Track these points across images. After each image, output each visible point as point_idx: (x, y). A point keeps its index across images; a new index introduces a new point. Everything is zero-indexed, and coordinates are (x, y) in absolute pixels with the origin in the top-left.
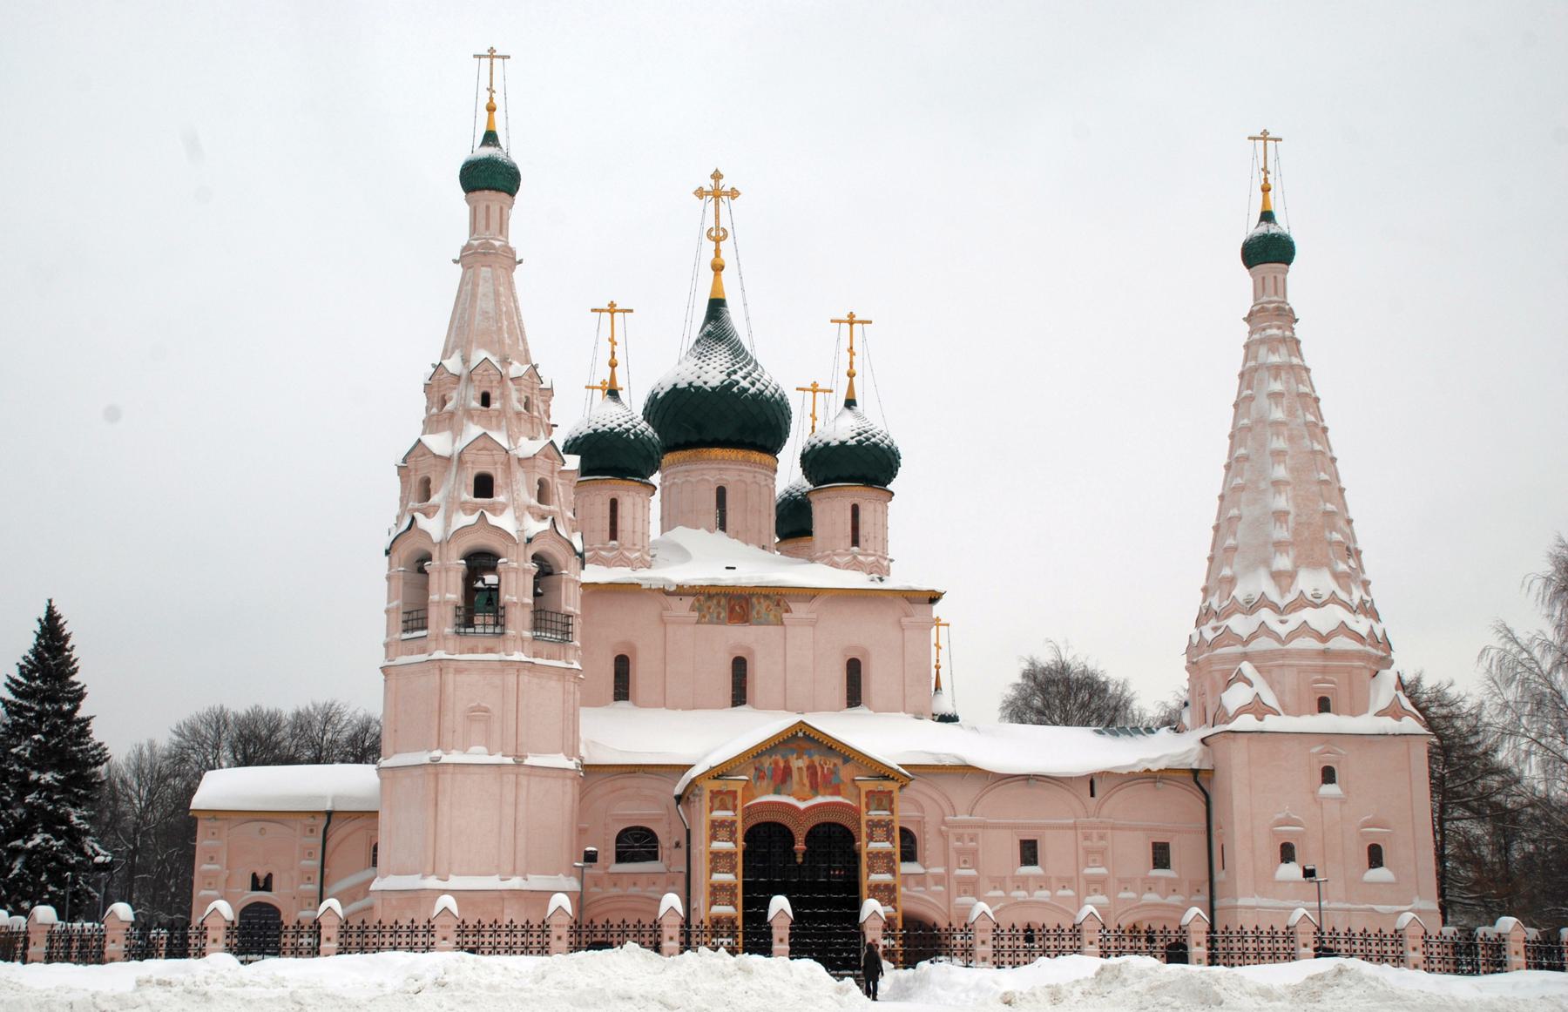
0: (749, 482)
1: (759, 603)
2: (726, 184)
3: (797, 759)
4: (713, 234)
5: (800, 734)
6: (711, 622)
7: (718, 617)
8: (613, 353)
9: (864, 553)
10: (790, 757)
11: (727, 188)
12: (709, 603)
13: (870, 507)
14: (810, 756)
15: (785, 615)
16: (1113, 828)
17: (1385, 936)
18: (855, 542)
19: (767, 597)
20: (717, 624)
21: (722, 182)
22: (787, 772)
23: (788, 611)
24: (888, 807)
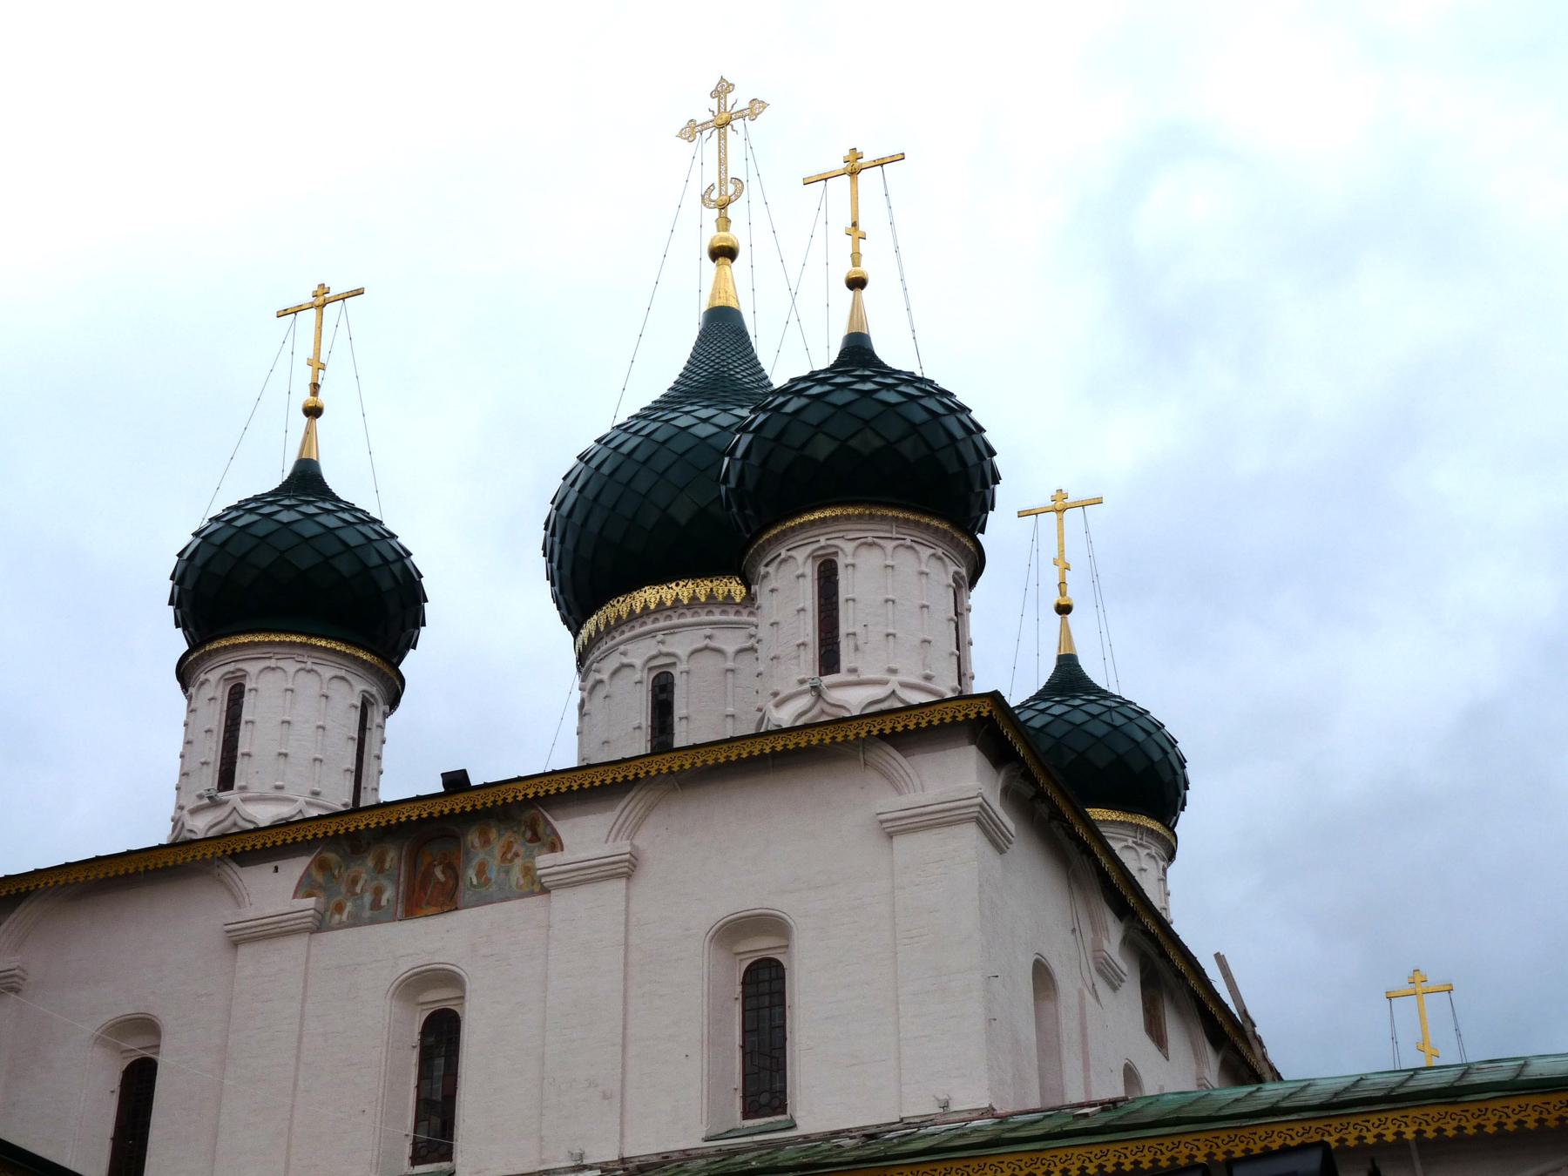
0: (730, 649)
1: (486, 842)
2: (739, 99)
4: (715, 195)
6: (355, 921)
8: (315, 388)
9: (852, 678)
11: (743, 104)
12: (355, 869)
15: (545, 861)
21: (731, 98)
23: (555, 845)
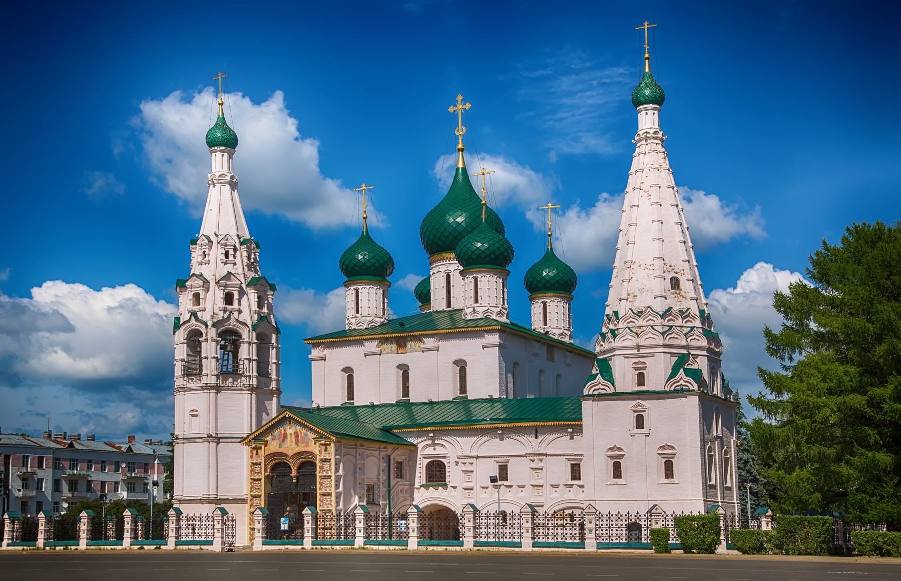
5: (287, 416)
6: (388, 353)
7: (392, 350)
10: (286, 428)
13: (485, 280)
15: (422, 346)
16: (546, 455)
17: (515, 515)
18: (476, 301)
20: (391, 353)
22: (285, 436)
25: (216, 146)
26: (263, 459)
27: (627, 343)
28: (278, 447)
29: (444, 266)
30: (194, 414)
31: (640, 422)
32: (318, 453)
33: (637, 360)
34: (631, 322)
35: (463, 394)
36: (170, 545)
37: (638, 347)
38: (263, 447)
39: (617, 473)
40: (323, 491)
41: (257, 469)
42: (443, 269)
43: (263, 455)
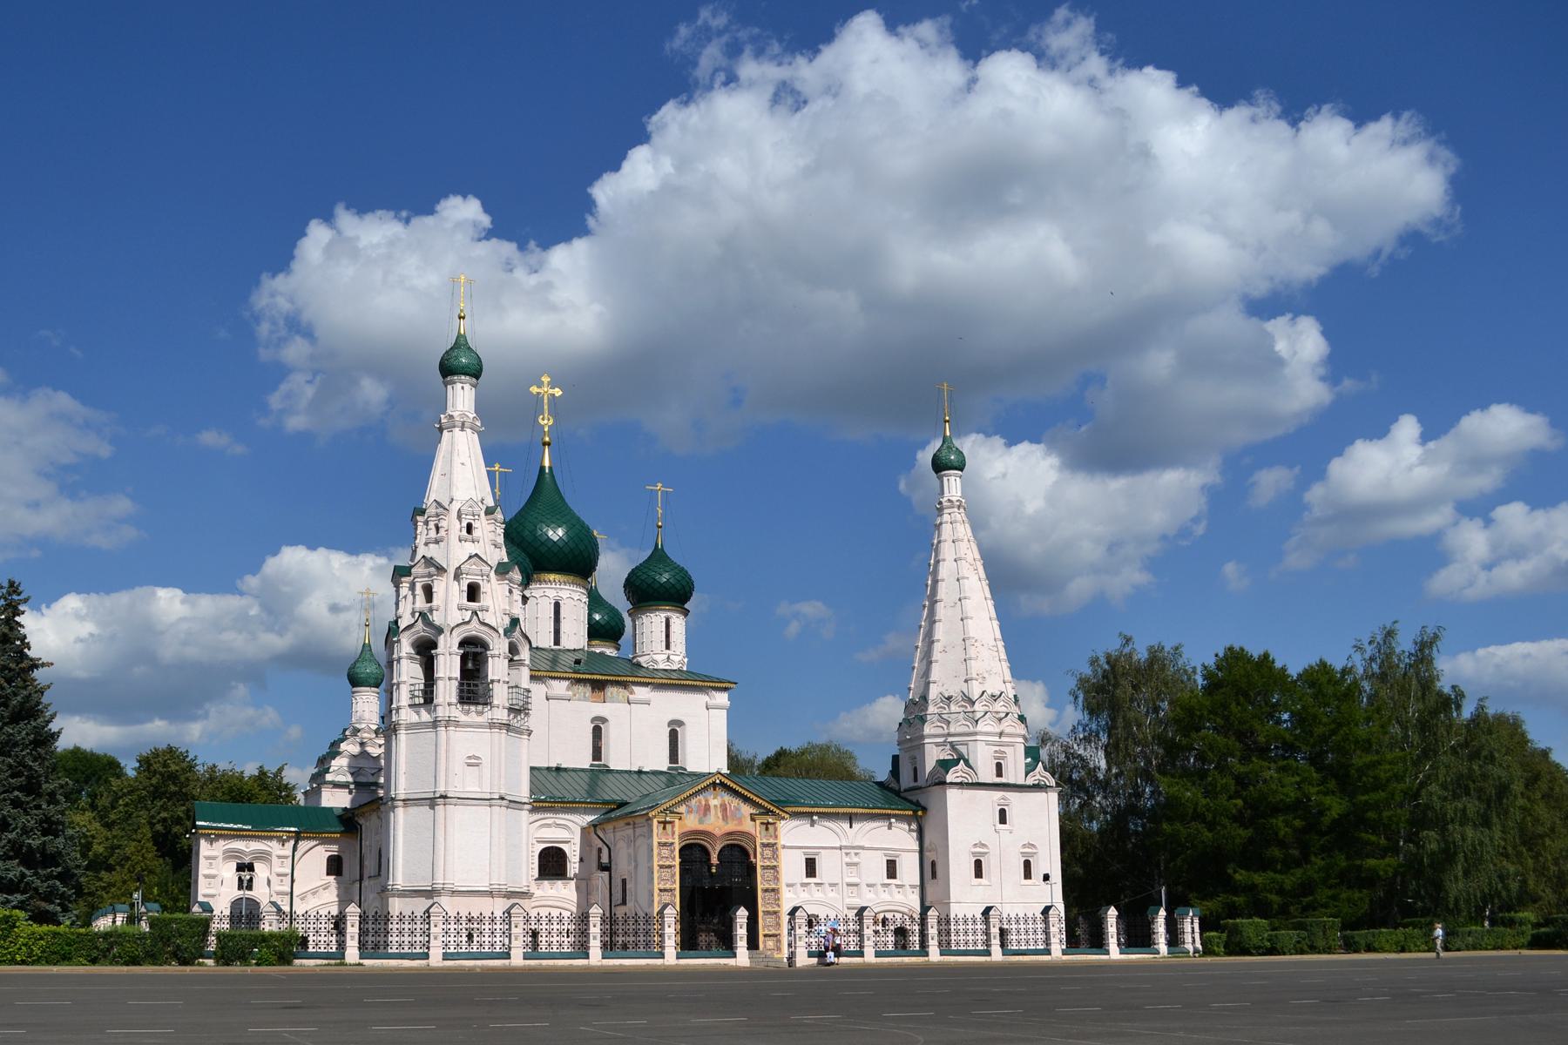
3: (714, 799)
5: (718, 781)
6: (579, 700)
10: (709, 797)
14: (722, 797)
15: (631, 697)
18: (668, 647)
19: (617, 683)
22: (707, 808)
23: (632, 692)
24: (773, 834)
25: (468, 375)
26: (676, 836)
27: (988, 729)
28: (697, 820)
29: (553, 590)
30: (473, 762)
31: (1003, 814)
32: (758, 834)
33: (997, 748)
34: (986, 705)
35: (674, 763)
36: (742, 958)
37: (1001, 734)
38: (677, 821)
39: (979, 874)
40: (767, 886)
41: (665, 852)
42: (552, 593)
43: (677, 834)
